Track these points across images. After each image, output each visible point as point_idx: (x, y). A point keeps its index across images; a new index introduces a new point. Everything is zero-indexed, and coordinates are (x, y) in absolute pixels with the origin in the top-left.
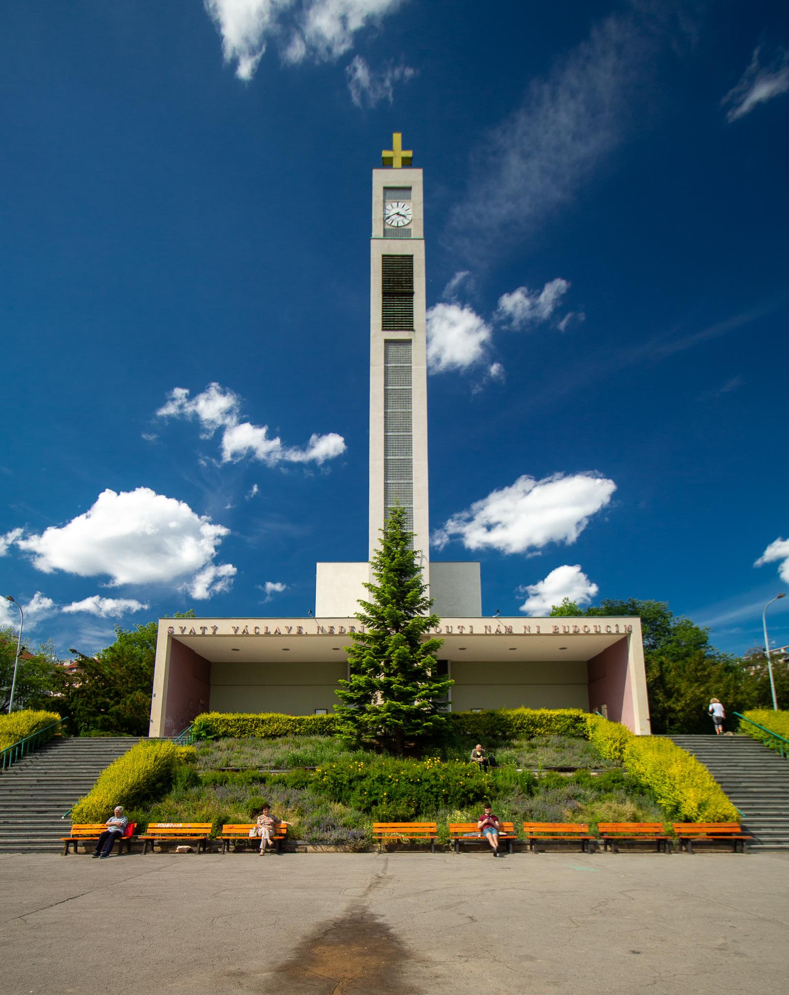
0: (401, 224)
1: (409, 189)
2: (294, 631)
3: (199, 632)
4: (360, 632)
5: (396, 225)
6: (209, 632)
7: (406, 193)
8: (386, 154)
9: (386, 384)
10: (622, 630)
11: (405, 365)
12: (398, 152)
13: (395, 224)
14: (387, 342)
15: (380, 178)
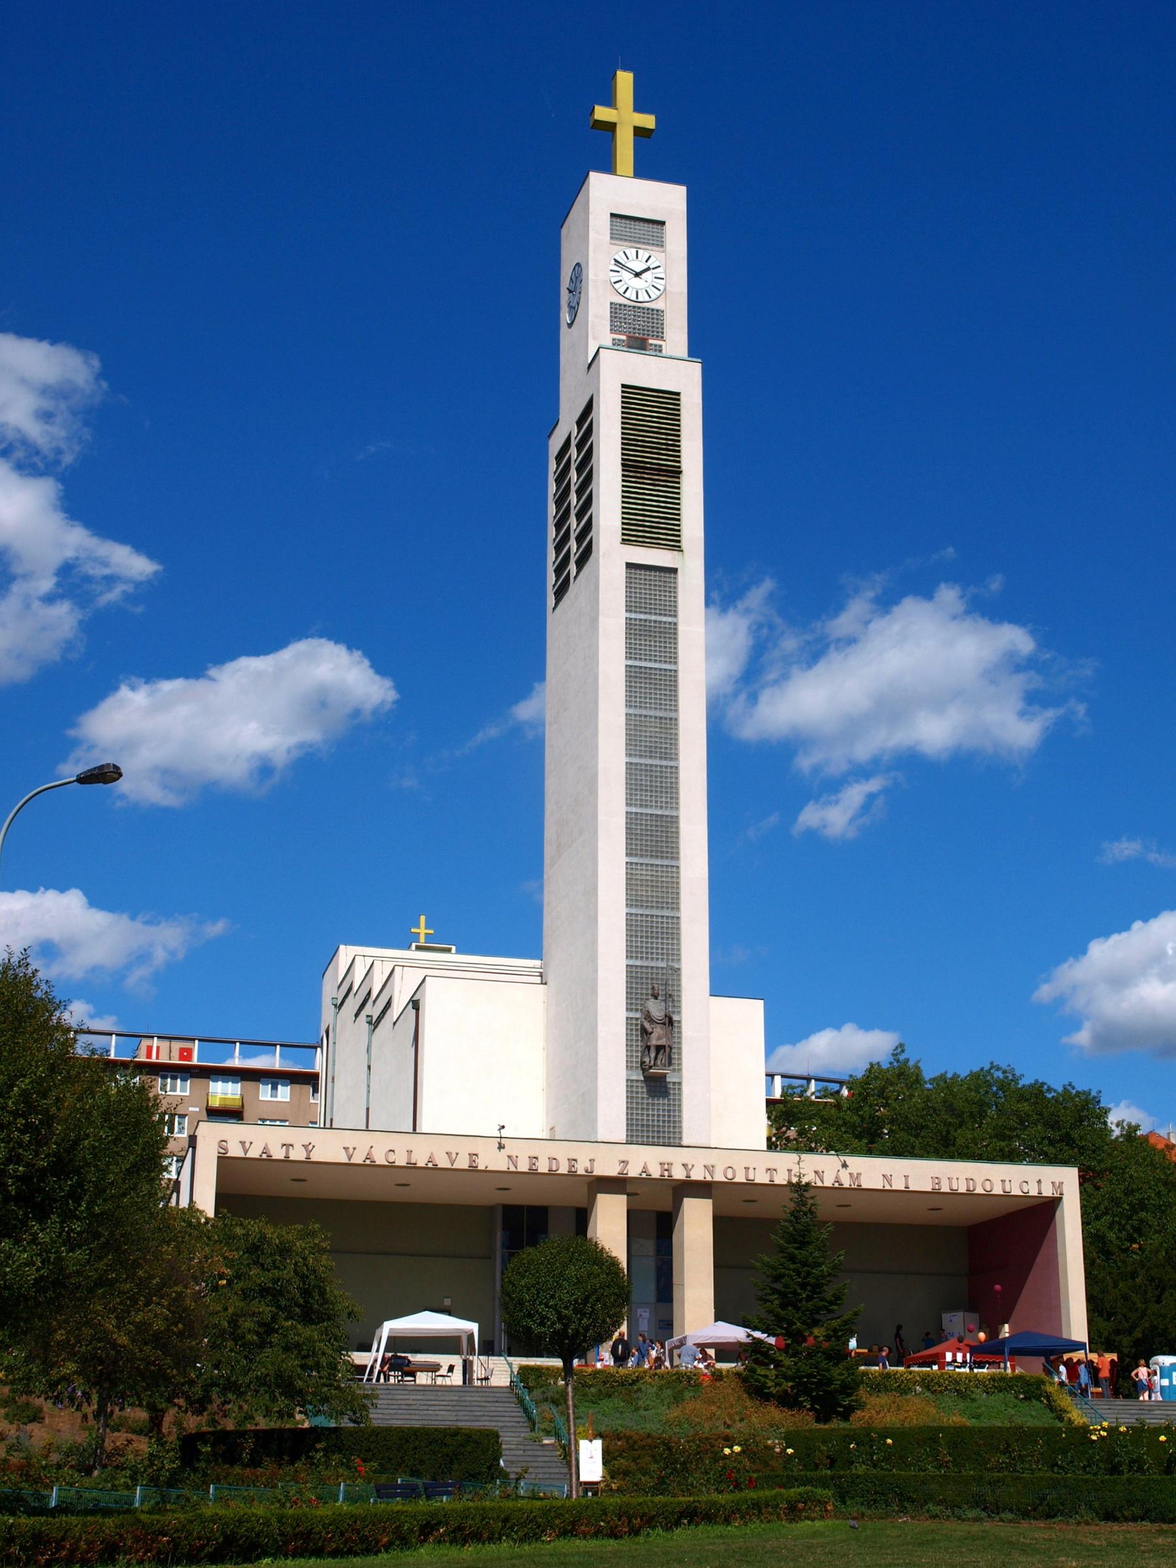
0: (643, 297)
1: (663, 223)
4: (587, 1171)
5: (634, 298)
11: (664, 619)
13: (631, 294)
14: (629, 566)
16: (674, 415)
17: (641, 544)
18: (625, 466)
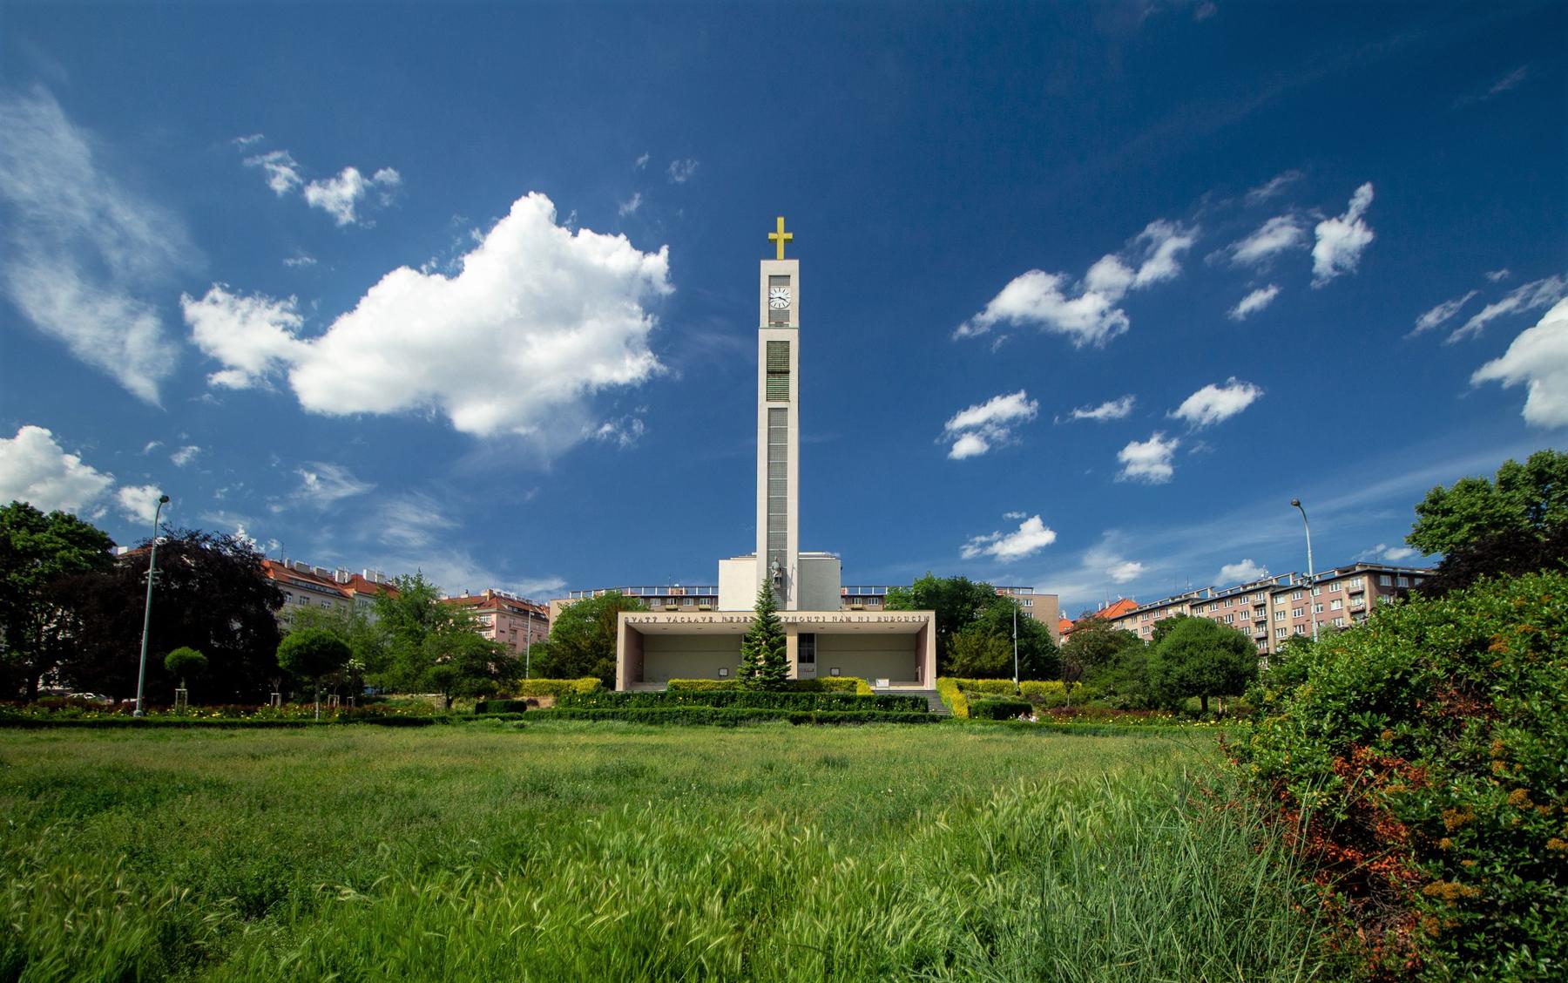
0: (782, 306)
2: (707, 620)
3: (645, 621)
6: (651, 621)
7: (786, 279)
8: (771, 236)
9: (769, 442)
10: (922, 620)
12: (781, 235)
13: (777, 306)
15: (768, 268)
16: (788, 350)
17: (775, 401)
18: (768, 372)
